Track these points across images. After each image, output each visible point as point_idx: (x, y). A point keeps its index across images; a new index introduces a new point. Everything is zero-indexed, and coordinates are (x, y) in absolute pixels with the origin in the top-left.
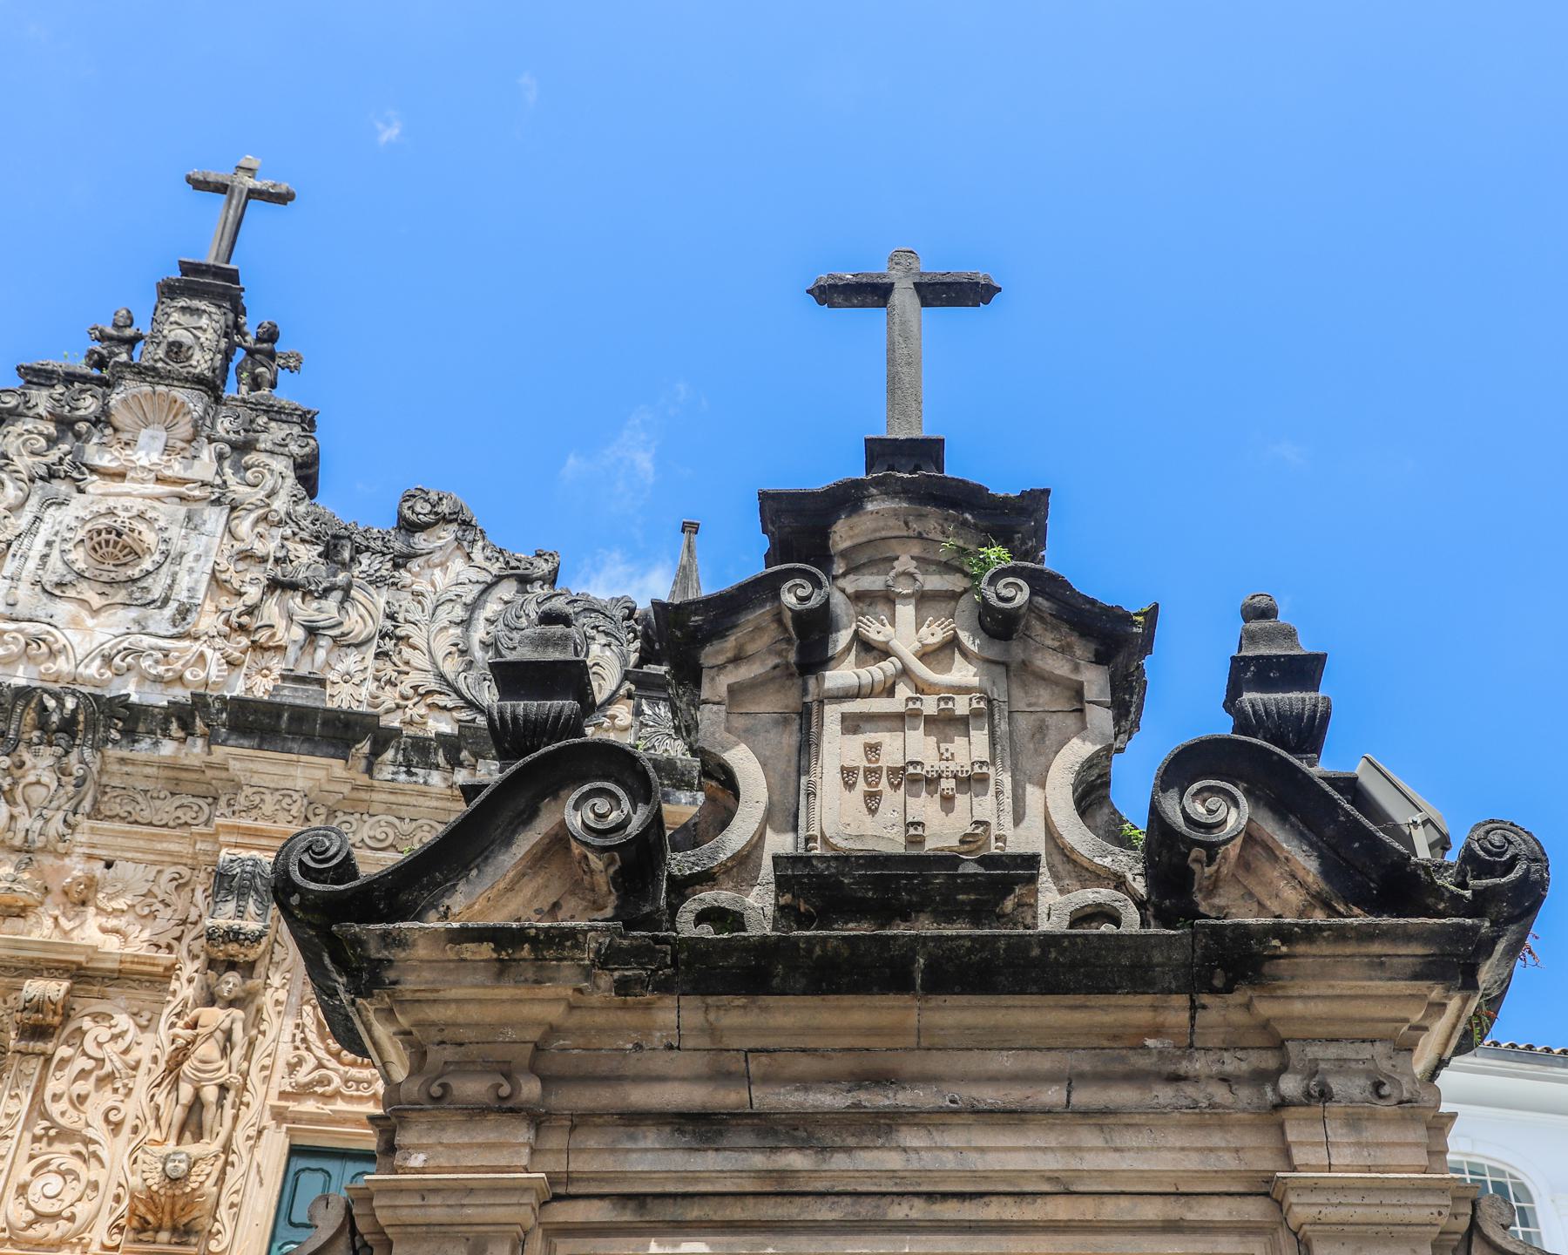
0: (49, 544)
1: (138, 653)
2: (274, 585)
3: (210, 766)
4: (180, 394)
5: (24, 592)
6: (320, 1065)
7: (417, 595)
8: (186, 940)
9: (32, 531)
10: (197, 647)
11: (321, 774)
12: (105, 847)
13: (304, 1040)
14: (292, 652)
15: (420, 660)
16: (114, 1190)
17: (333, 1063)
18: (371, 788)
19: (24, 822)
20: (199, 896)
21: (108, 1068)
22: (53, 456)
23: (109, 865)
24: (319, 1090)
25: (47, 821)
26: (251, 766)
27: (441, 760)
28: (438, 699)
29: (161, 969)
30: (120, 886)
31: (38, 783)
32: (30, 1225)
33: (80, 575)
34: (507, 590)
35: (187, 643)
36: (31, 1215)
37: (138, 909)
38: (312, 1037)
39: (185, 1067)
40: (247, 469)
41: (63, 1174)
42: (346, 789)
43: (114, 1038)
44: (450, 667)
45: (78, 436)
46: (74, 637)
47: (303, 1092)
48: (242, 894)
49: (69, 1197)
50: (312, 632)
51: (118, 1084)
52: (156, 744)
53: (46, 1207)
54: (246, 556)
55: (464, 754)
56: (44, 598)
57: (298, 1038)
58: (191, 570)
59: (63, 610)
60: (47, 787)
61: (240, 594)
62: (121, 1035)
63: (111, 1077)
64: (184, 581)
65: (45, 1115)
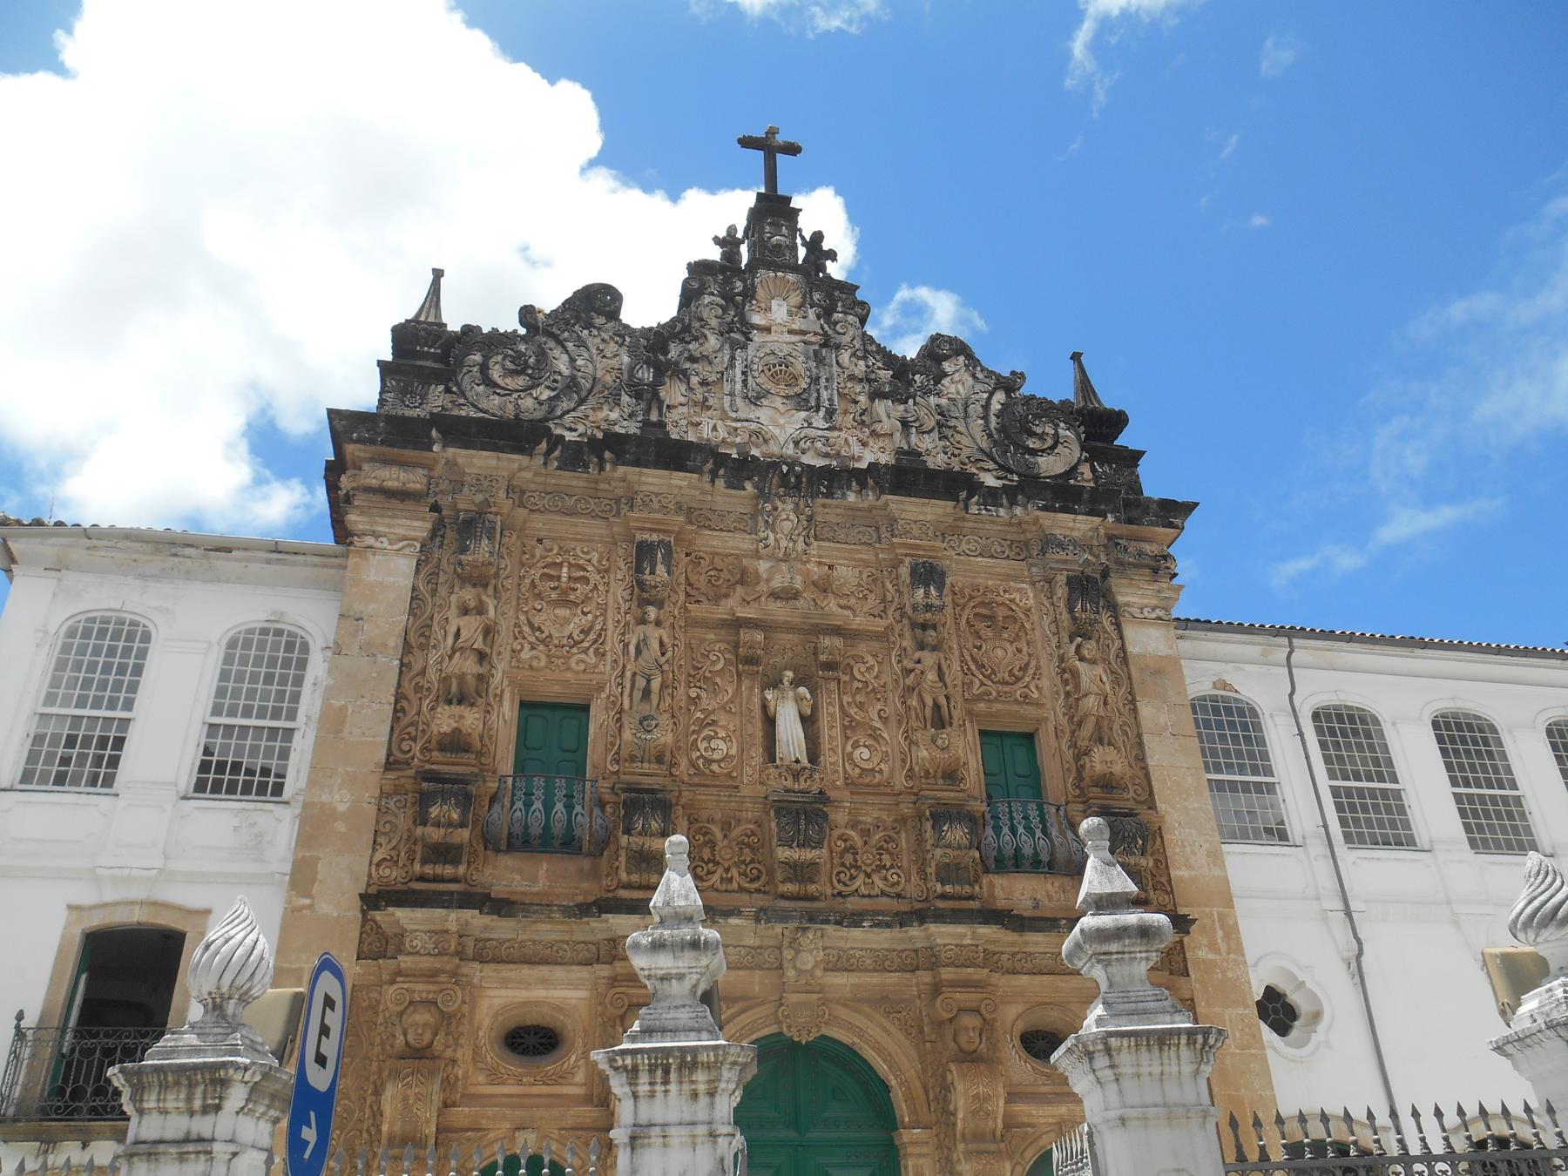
0: (744, 373)
1: (813, 440)
2: (876, 395)
3: (875, 507)
4: (791, 277)
5: (739, 402)
6: (983, 684)
8: (890, 612)
9: (731, 366)
10: (843, 435)
11: (940, 511)
14: (897, 435)
15: (965, 441)
16: (898, 756)
18: (964, 519)
19: (784, 543)
20: (889, 586)
22: (729, 319)
23: (831, 567)
27: (1005, 501)
28: (981, 464)
34: (1000, 396)
35: (836, 434)
38: (973, 667)
40: (836, 323)
42: (950, 520)
44: (984, 445)
45: (736, 306)
46: (777, 431)
47: (979, 698)
48: (927, 586)
49: (876, 760)
50: (905, 424)
54: (852, 378)
59: (763, 414)
61: (856, 402)
63: (873, 690)
64: (825, 395)
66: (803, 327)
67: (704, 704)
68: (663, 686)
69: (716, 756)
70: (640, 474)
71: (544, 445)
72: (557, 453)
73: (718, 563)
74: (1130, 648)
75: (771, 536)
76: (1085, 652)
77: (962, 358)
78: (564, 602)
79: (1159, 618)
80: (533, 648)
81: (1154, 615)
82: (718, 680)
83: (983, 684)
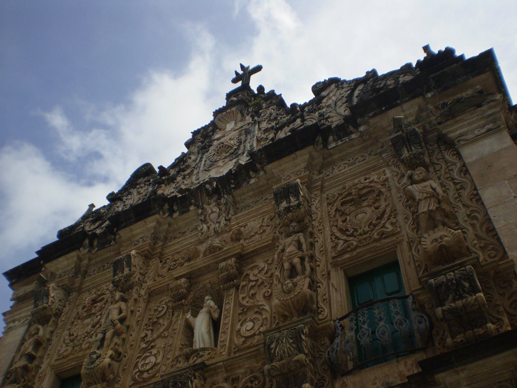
0: (205, 161)
3: (268, 179)
7: (328, 106)
12: (242, 221)
13: (336, 238)
17: (351, 238)
18: (331, 155)
21: (260, 281)
24: (349, 249)
25: (219, 223)
26: (281, 168)
27: (351, 128)
29: (271, 242)
30: (250, 229)
31: (213, 212)
32: (244, 342)
33: (216, 161)
36: (243, 339)
37: (259, 232)
39: (284, 258)
41: (252, 321)
43: (260, 272)
51: (266, 284)
52: (248, 182)
53: (248, 334)
55: (359, 120)
56: (207, 172)
57: (333, 239)
58: (249, 142)
60: (216, 212)
62: (263, 269)
63: (263, 283)
65: (241, 305)
66: (242, 125)
67: (149, 338)
68: (117, 333)
69: (148, 367)
70: (132, 231)
71: (87, 242)
72: (95, 243)
73: (176, 257)
74: (467, 161)
75: (205, 227)
76: (416, 177)
77: (333, 86)
78: (89, 316)
79: (489, 130)
80: (67, 346)
81: (484, 130)
82: (161, 321)
83: (346, 241)
